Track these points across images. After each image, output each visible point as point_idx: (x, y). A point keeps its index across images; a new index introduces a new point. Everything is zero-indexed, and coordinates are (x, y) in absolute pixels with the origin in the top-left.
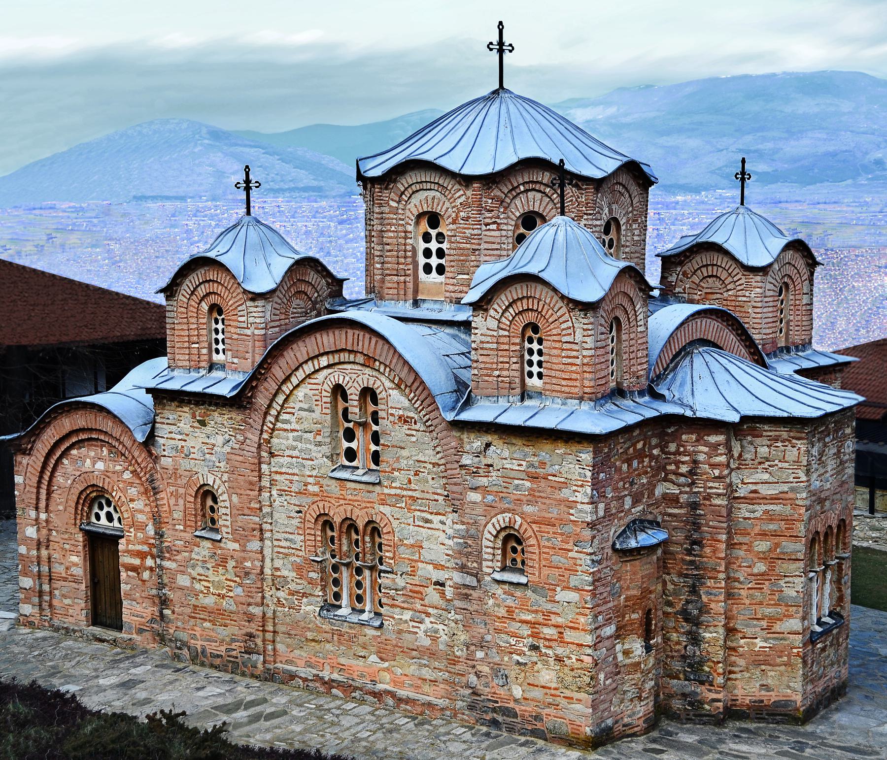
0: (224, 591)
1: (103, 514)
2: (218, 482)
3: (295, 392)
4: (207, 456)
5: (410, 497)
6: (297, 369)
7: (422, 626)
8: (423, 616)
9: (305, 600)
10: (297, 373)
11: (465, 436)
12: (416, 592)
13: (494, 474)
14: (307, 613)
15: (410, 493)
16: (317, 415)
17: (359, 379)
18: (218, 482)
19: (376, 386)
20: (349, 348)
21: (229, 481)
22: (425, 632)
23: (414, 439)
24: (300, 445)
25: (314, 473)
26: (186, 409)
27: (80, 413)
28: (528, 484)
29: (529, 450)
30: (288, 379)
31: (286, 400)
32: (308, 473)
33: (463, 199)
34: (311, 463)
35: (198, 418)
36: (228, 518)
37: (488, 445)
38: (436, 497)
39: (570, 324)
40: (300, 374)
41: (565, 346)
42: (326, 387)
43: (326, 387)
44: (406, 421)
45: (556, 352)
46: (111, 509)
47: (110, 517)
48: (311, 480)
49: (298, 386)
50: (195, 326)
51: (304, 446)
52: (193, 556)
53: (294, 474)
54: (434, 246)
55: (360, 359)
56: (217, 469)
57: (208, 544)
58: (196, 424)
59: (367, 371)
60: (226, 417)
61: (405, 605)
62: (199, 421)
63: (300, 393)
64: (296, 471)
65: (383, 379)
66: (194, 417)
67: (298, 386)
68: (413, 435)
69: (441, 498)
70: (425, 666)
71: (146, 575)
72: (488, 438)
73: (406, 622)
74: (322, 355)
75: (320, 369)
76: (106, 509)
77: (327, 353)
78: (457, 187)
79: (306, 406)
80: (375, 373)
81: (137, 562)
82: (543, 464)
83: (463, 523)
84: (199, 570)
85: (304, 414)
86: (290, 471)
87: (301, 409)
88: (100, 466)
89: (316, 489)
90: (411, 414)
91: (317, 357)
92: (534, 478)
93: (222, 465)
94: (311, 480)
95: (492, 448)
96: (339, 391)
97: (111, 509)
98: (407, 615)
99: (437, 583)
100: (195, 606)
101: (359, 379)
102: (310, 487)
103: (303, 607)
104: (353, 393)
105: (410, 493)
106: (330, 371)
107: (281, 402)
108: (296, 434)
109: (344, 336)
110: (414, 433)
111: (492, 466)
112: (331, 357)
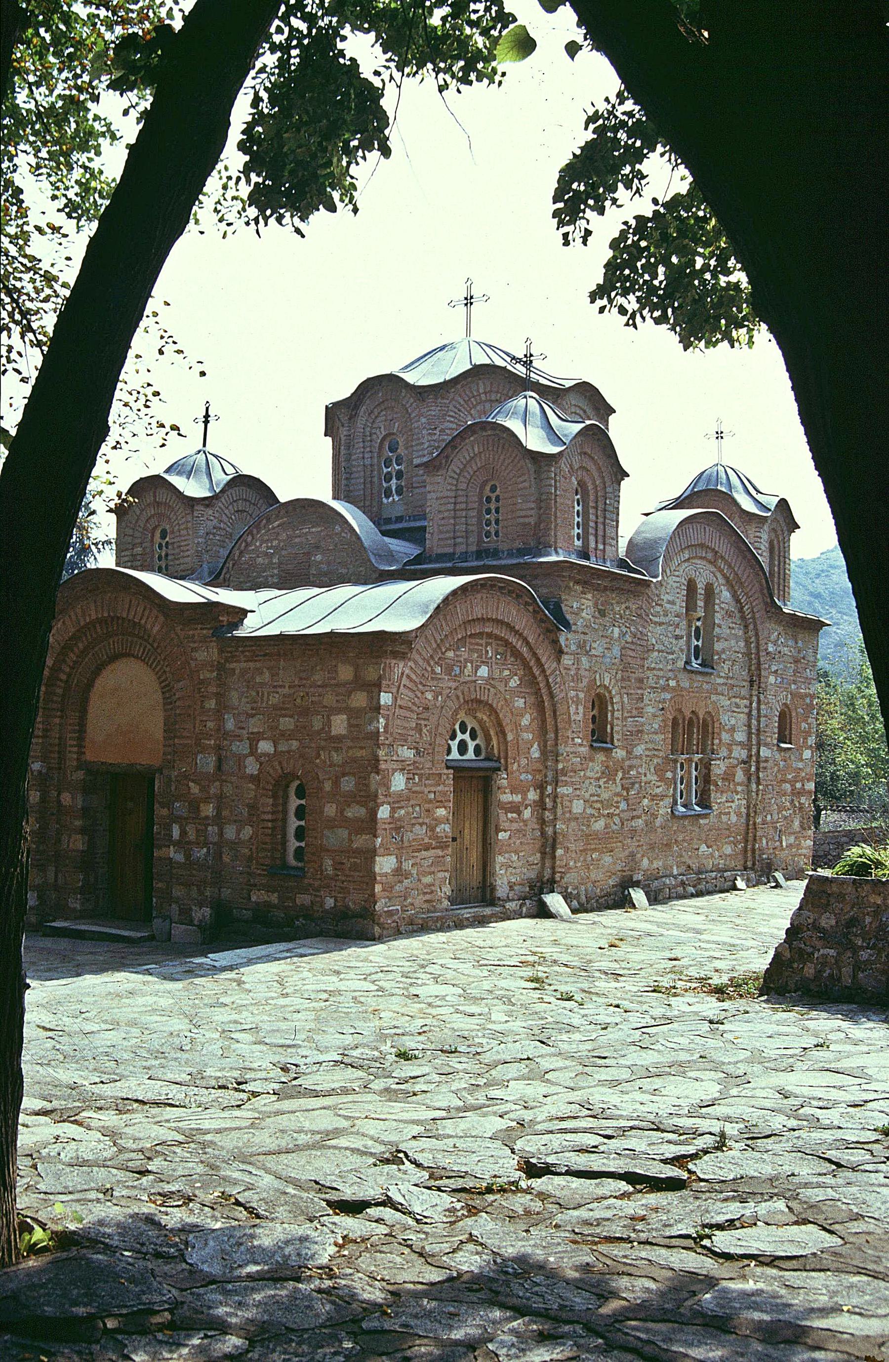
1: (454, 745)
21: (623, 679)
26: (589, 596)
27: (479, 596)
47: (463, 747)
52: (589, 774)
60: (623, 606)
66: (596, 605)
71: (527, 813)
76: (460, 736)
81: (517, 798)
84: (592, 789)
85: (668, 606)
88: (483, 671)
96: (691, 586)
97: (467, 737)
100: (588, 835)
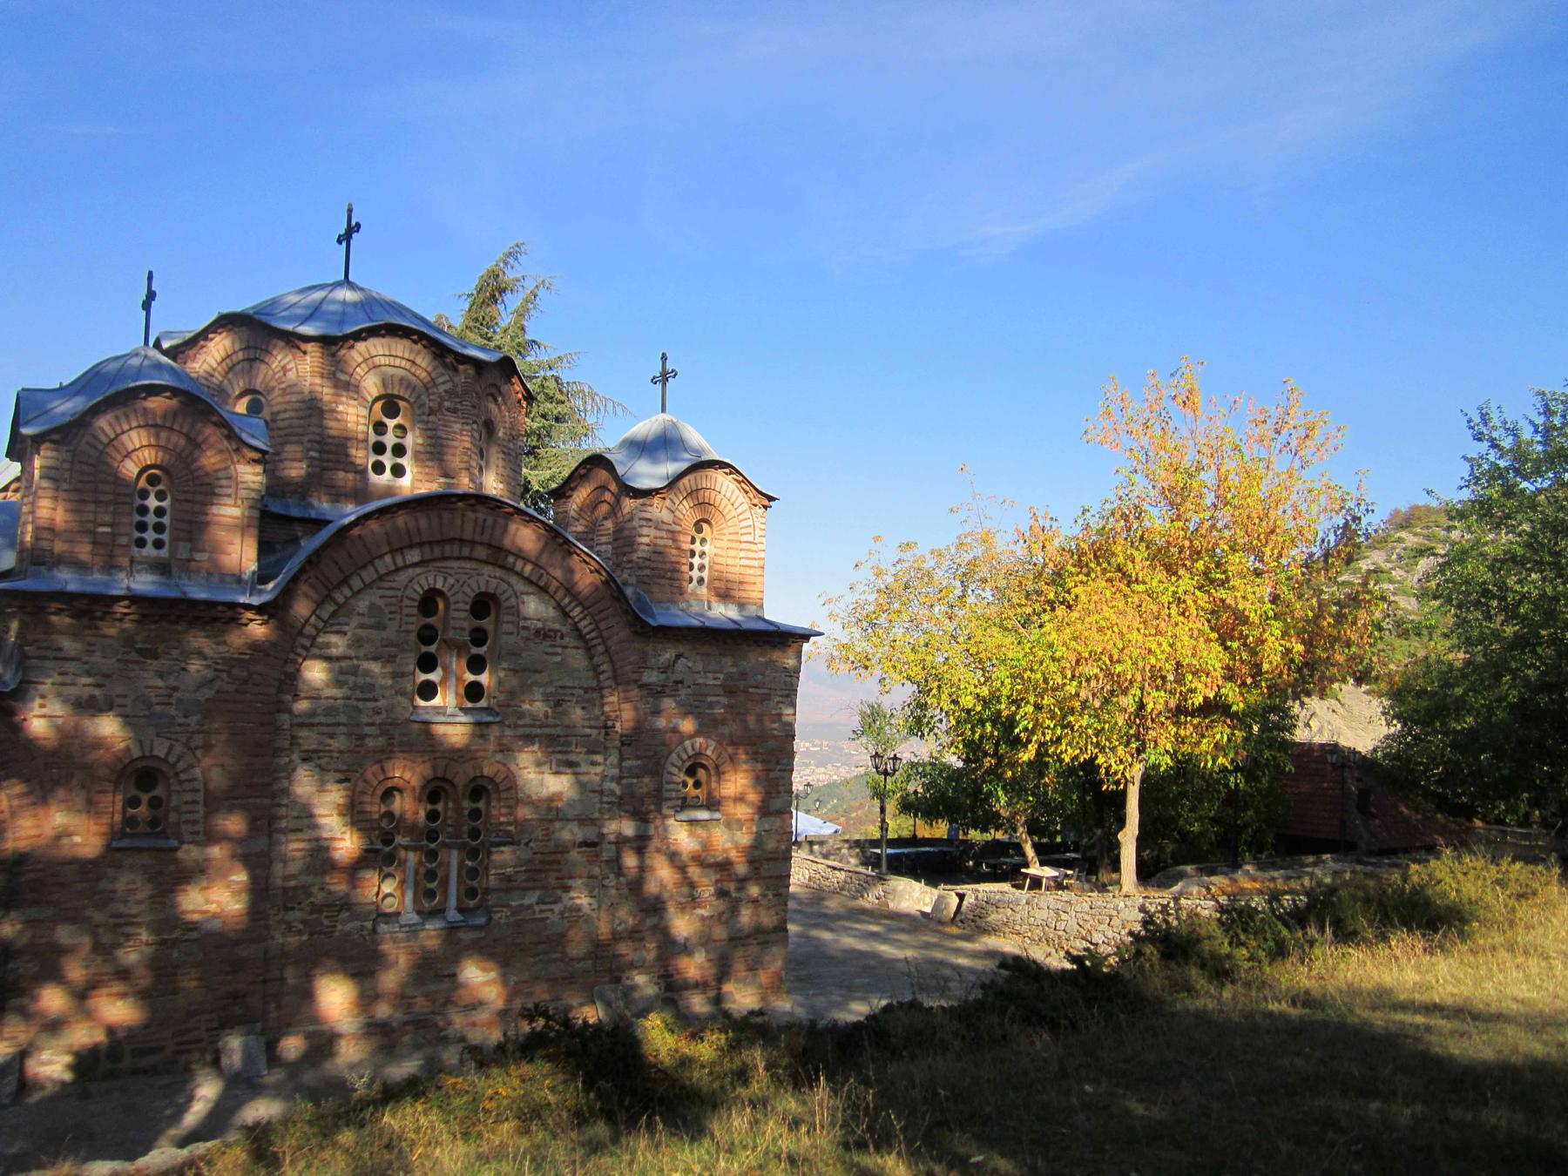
0: (177, 933)
2: (178, 749)
3: (352, 601)
4: (158, 708)
5: (548, 736)
6: (364, 567)
7: (557, 908)
8: (559, 892)
9: (345, 915)
10: (364, 574)
11: (649, 649)
12: (549, 863)
13: (683, 692)
14: (348, 934)
15: (547, 731)
16: (391, 632)
17: (472, 582)
18: (178, 749)
19: (499, 591)
20: (468, 535)
22: (562, 913)
23: (558, 659)
24: (352, 679)
25: (378, 719)
28: (724, 700)
29: (728, 661)
30: (345, 581)
31: (333, 615)
32: (365, 720)
33: (448, 386)
34: (372, 704)
35: (139, 646)
36: (200, 807)
37: (678, 657)
38: (588, 731)
39: (749, 522)
40: (369, 575)
41: (743, 546)
42: (409, 592)
43: (409, 592)
44: (546, 636)
45: (732, 553)
48: (367, 730)
49: (359, 591)
50: (111, 497)
51: (361, 680)
53: (338, 724)
56: (178, 729)
57: (146, 859)
58: (134, 656)
59: (487, 570)
61: (530, 884)
62: (139, 651)
63: (362, 604)
64: (343, 719)
65: (514, 580)
67: (359, 591)
68: (556, 654)
69: (594, 732)
70: (555, 961)
72: (681, 649)
73: (530, 907)
74: (411, 546)
75: (406, 567)
77: (421, 545)
78: (441, 369)
79: (372, 621)
80: (499, 572)
82: (743, 675)
83: (638, 758)
85: (364, 633)
86: (330, 720)
87: (362, 626)
89: (381, 742)
90: (557, 626)
91: (401, 550)
92: (730, 692)
93: (193, 720)
94: (367, 730)
95: (682, 660)
98: (532, 898)
99: (585, 844)
101: (472, 582)
102: (370, 743)
103: (340, 927)
105: (547, 731)
106: (418, 570)
107: (325, 615)
108: (344, 664)
109: (458, 522)
110: (559, 650)
111: (681, 682)
112: (427, 549)
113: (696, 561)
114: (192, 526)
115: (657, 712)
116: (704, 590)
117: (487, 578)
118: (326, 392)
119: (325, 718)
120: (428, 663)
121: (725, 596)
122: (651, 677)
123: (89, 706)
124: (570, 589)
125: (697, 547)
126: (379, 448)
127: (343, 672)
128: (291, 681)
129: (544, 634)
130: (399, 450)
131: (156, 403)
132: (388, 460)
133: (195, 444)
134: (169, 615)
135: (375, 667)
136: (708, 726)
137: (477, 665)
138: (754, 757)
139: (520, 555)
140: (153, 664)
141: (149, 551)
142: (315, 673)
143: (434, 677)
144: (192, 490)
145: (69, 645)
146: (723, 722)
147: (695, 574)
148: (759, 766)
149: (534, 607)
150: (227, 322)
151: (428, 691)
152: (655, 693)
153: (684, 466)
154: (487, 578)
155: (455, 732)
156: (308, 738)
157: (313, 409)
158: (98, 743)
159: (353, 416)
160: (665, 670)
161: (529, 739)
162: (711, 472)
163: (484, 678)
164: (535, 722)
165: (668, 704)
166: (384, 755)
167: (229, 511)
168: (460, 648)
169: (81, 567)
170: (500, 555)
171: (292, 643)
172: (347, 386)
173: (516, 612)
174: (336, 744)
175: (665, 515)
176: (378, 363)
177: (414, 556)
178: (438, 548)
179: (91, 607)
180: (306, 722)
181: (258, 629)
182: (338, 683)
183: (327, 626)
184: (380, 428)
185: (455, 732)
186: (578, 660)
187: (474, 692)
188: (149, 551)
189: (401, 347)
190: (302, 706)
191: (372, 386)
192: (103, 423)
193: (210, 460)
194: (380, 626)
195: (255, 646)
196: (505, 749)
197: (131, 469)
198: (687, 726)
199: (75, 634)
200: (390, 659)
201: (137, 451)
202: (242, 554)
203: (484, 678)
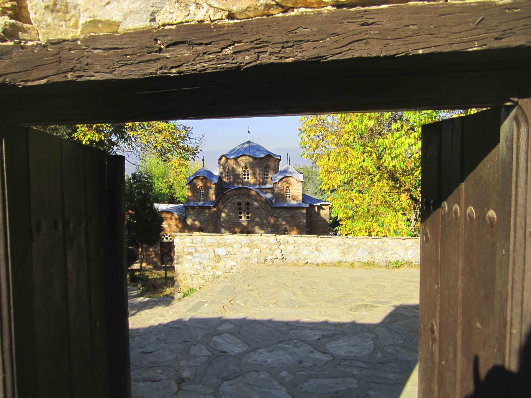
40: (229, 200)
46: (168, 237)
54: (246, 173)
55: (246, 196)
63: (228, 205)
82: (294, 214)
104: (243, 204)
113: (288, 193)
114: (207, 194)
115: (277, 221)
116: (290, 199)
117: (248, 200)
118: (235, 167)
119: (225, 221)
120: (240, 213)
121: (294, 199)
122: (275, 215)
123: (194, 220)
124: (261, 200)
125: (288, 191)
126: (245, 175)
127: (227, 215)
128: (219, 216)
129: (257, 208)
130: (248, 175)
131: (201, 177)
132: (246, 176)
133: (206, 183)
134: (203, 208)
135: (231, 214)
136: (288, 223)
137: (248, 213)
138: (297, 229)
139: (252, 195)
140: (202, 215)
141: (202, 198)
142: (223, 215)
143: (242, 215)
144: (207, 188)
145: (192, 212)
146: (291, 222)
147: (288, 196)
148: (298, 230)
149: (256, 204)
150: (223, 156)
151: (241, 217)
152: (277, 218)
153: (282, 177)
154: (248, 200)
155: (245, 223)
156: (223, 224)
157: (233, 169)
158: (196, 225)
159: (240, 170)
160: (278, 214)
161: (256, 225)
162: (289, 178)
163: (250, 215)
164: (257, 222)
165: (280, 219)
166: (235, 226)
167: (212, 192)
168: (245, 211)
169: (194, 202)
170: (249, 196)
171: (220, 211)
172: (238, 165)
173: (253, 205)
174: (227, 226)
175: (280, 186)
176: (243, 160)
177: (236, 197)
178: (239, 196)
179: (193, 208)
180: (222, 222)
181: (214, 209)
182: (226, 216)
183: (223, 208)
184: (245, 171)
185: (245, 223)
186: (264, 212)
187: (248, 217)
188: (202, 198)
189: (247, 158)
190: (222, 220)
191: (243, 164)
192: (195, 181)
193: (208, 184)
194: (231, 208)
195: (214, 211)
196: (253, 227)
197: (198, 187)
198: (284, 223)
199: (192, 211)
200: (233, 213)
201: (200, 184)
202: (213, 197)
203: (250, 215)
